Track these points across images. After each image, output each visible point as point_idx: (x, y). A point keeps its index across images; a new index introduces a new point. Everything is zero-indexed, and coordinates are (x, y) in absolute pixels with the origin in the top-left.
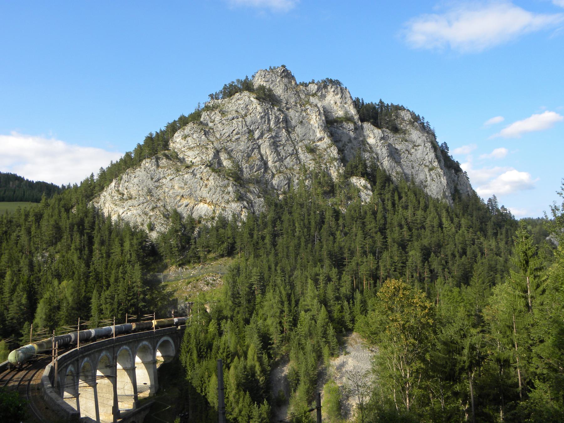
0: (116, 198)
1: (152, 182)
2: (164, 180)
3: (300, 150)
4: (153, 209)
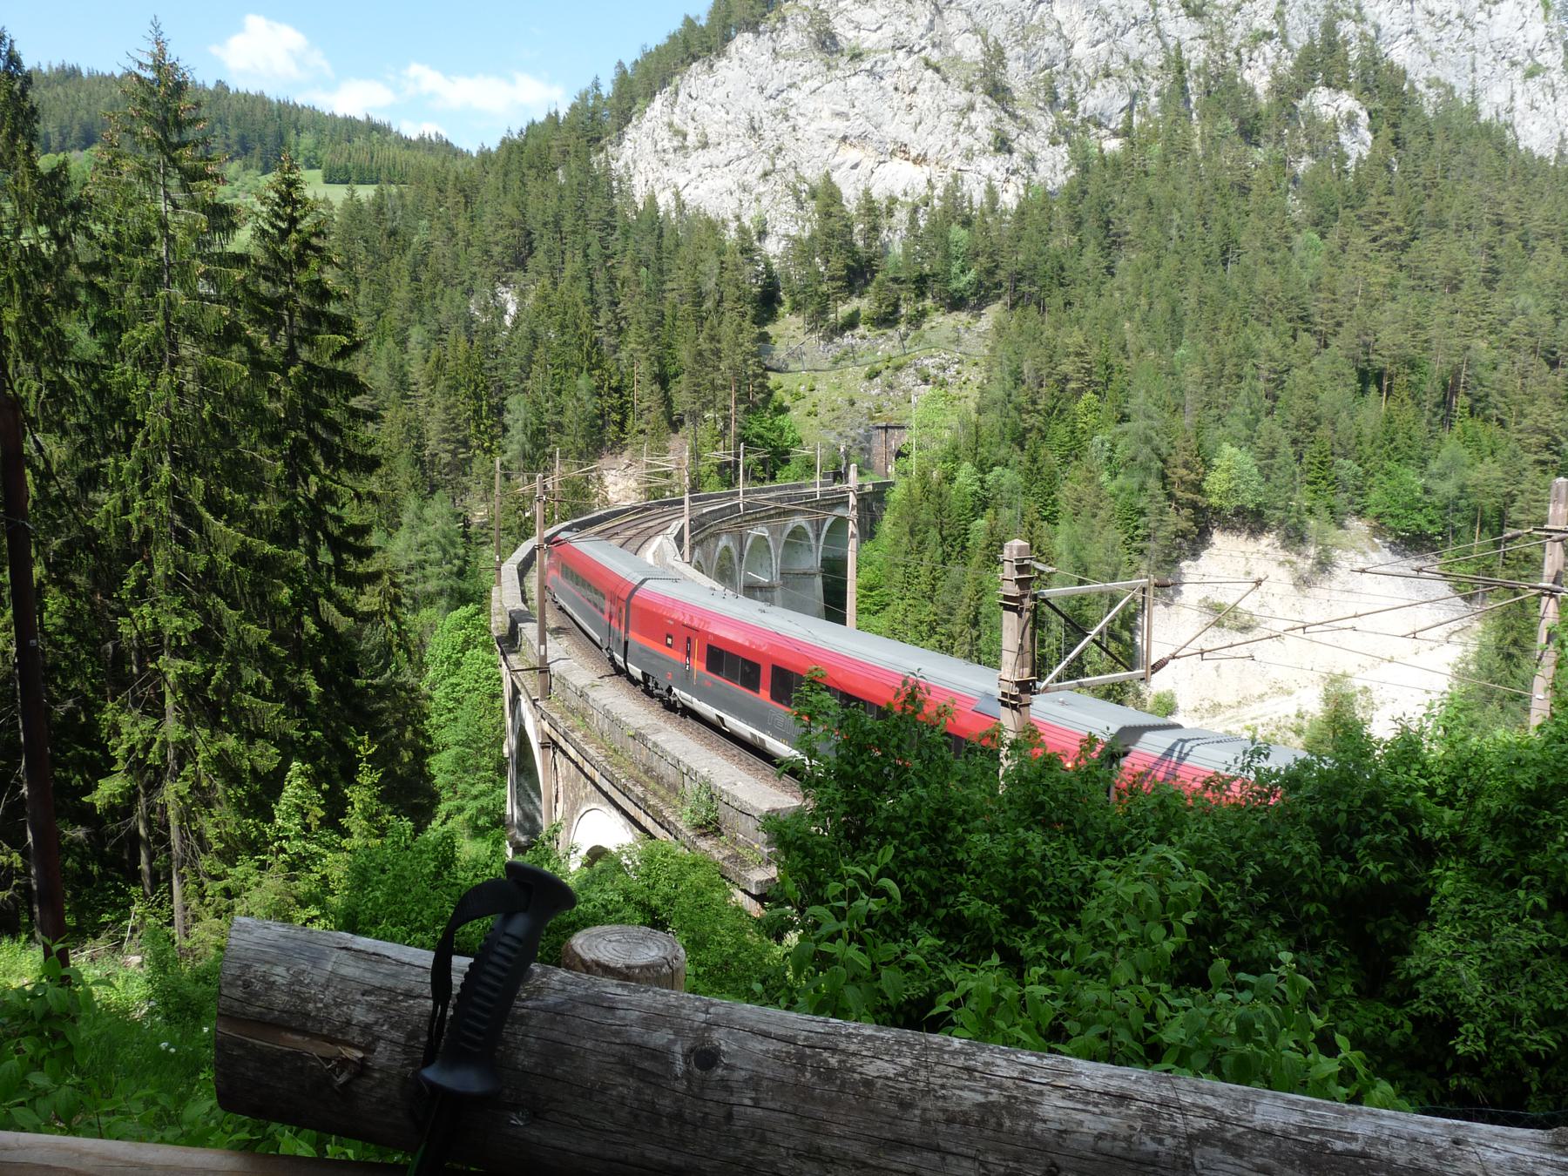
0: (667, 145)
1: (761, 100)
2: (793, 94)
3: (1164, 10)
4: (766, 174)
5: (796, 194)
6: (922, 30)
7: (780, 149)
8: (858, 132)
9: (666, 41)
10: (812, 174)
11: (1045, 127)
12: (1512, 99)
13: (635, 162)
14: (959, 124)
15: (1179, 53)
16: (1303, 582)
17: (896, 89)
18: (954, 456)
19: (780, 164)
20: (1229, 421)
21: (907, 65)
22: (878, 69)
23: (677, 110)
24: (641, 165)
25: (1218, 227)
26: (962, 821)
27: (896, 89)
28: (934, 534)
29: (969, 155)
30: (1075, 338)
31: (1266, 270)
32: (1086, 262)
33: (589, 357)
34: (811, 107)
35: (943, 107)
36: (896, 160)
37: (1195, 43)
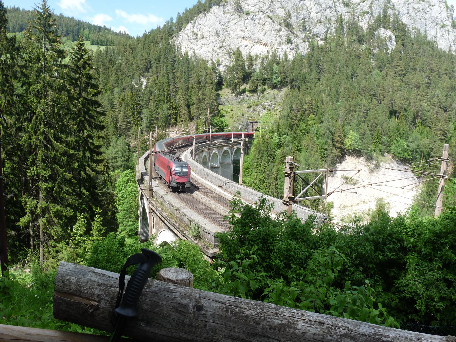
1: (220, 25)
2: (229, 24)
3: (337, 4)
4: (220, 47)
5: (229, 53)
6: (267, 7)
7: (225, 40)
8: (247, 36)
9: (192, 7)
10: (234, 48)
11: (302, 37)
12: (436, 34)
13: (182, 42)
14: (277, 35)
15: (341, 17)
16: (371, 171)
17: (259, 24)
18: (272, 131)
19: (224, 44)
20: (352, 124)
21: (262, 17)
22: (254, 18)
23: (195, 27)
24: (184, 43)
25: (351, 68)
26: (272, 237)
27: (259, 24)
28: (265, 154)
29: (279, 44)
30: (308, 98)
31: (364, 81)
32: (312, 76)
33: (167, 99)
34: (234, 28)
35: (273, 29)
36: (258, 44)
37: (346, 14)
